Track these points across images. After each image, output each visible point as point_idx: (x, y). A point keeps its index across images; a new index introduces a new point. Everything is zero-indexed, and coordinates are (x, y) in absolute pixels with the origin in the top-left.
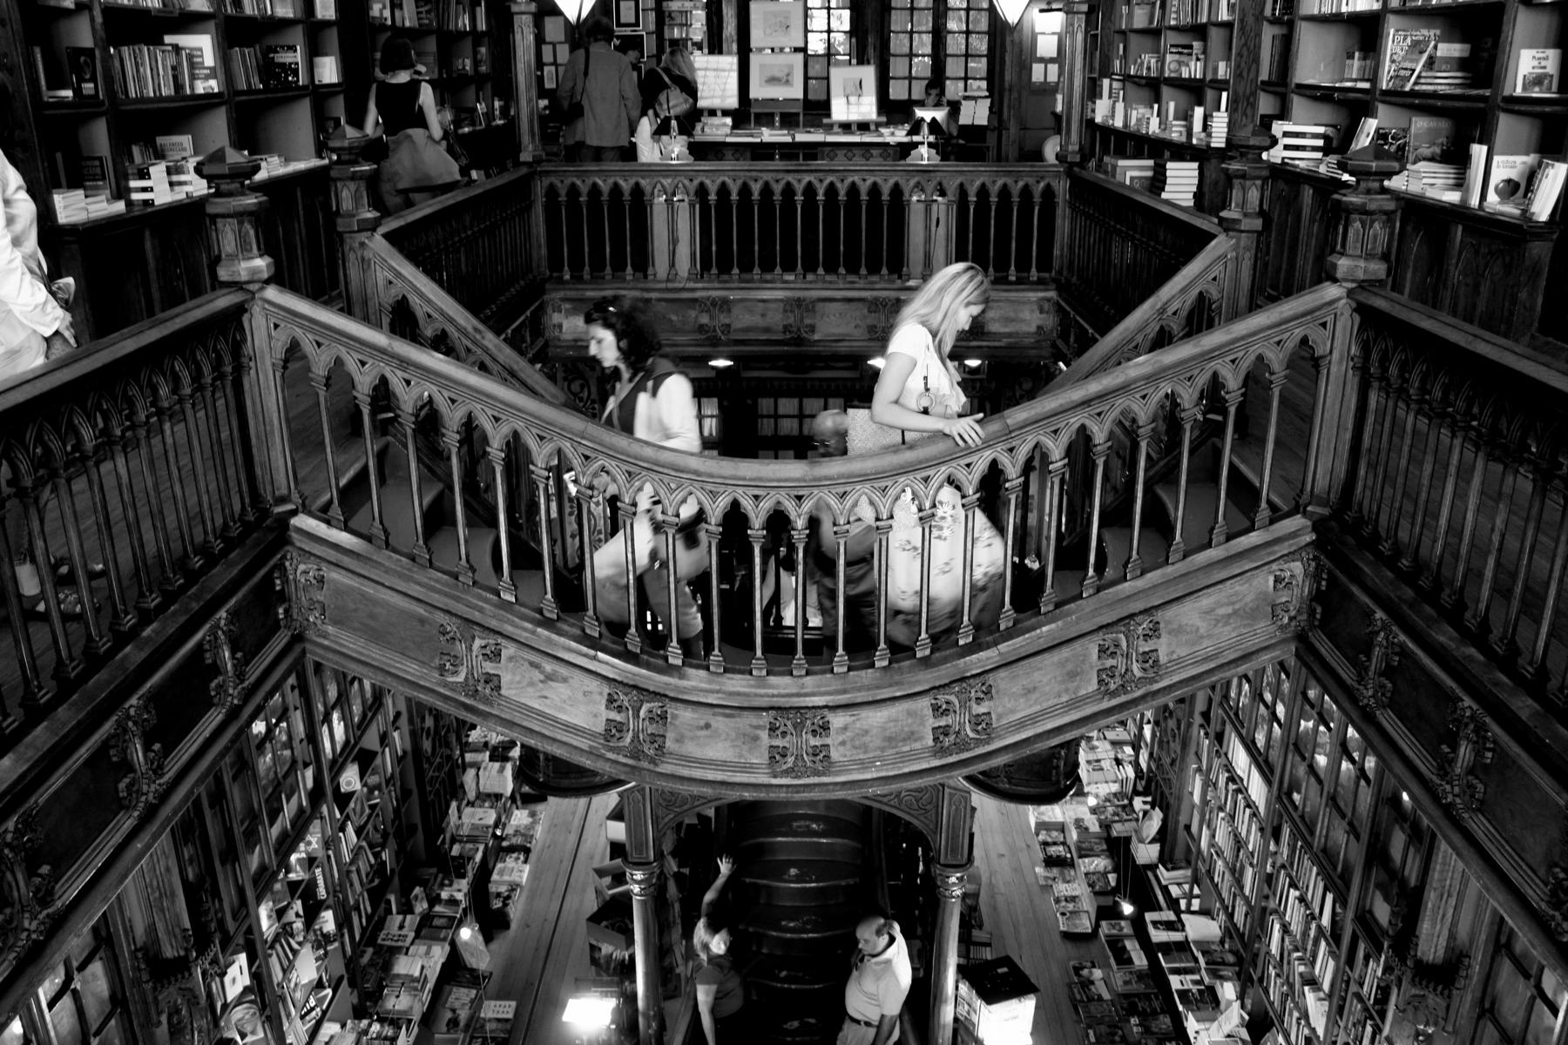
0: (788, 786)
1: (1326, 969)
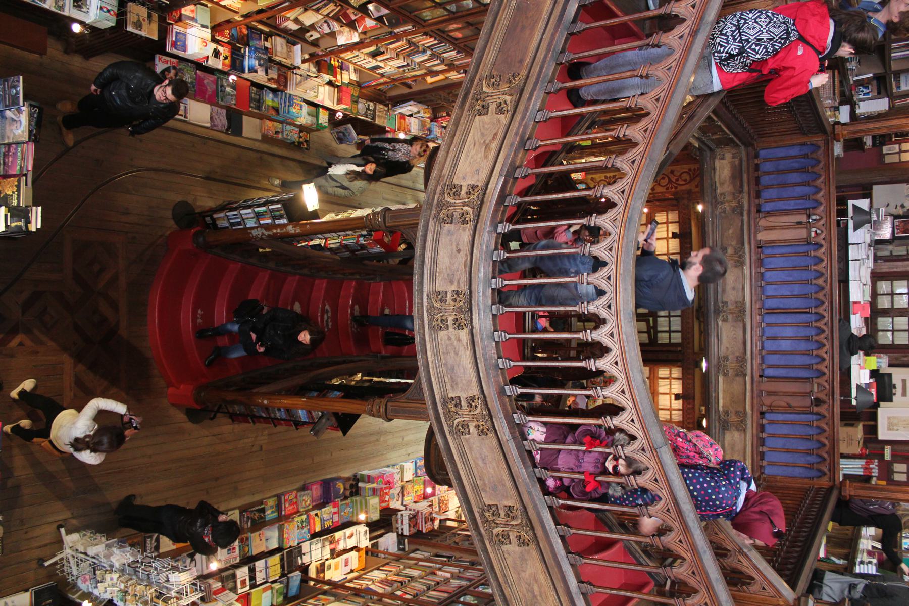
0: (422, 304)
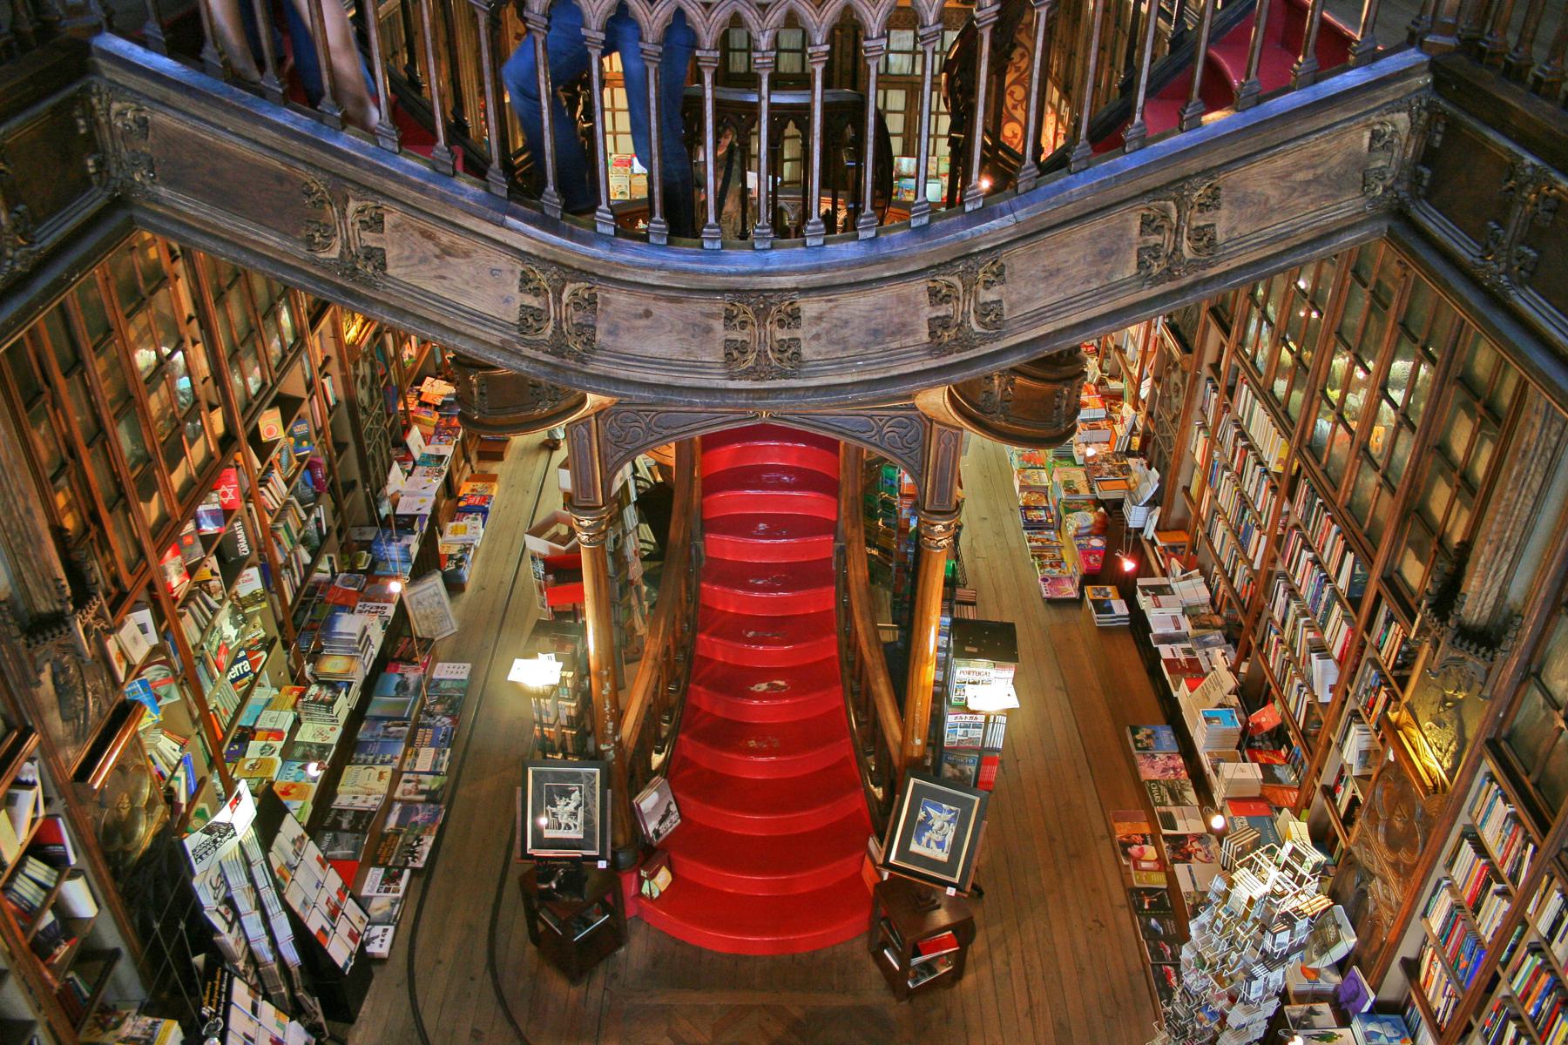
1: (1338, 633)
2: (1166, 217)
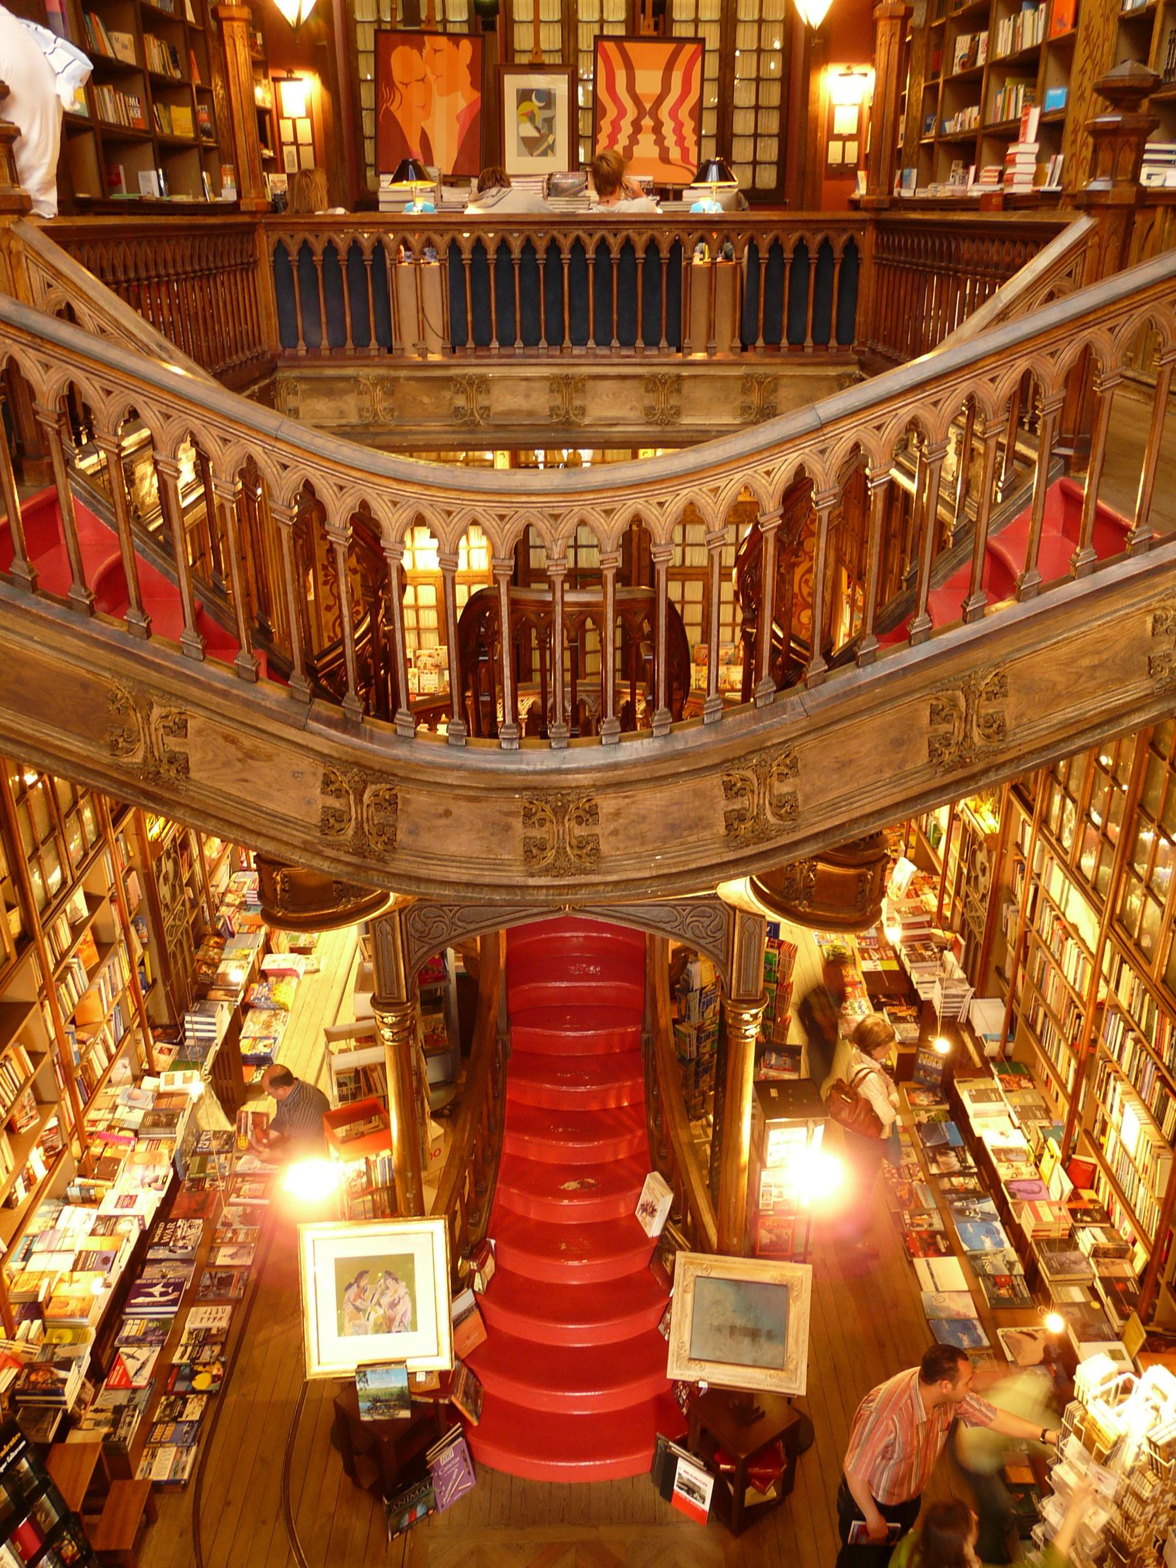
2: (955, 706)
